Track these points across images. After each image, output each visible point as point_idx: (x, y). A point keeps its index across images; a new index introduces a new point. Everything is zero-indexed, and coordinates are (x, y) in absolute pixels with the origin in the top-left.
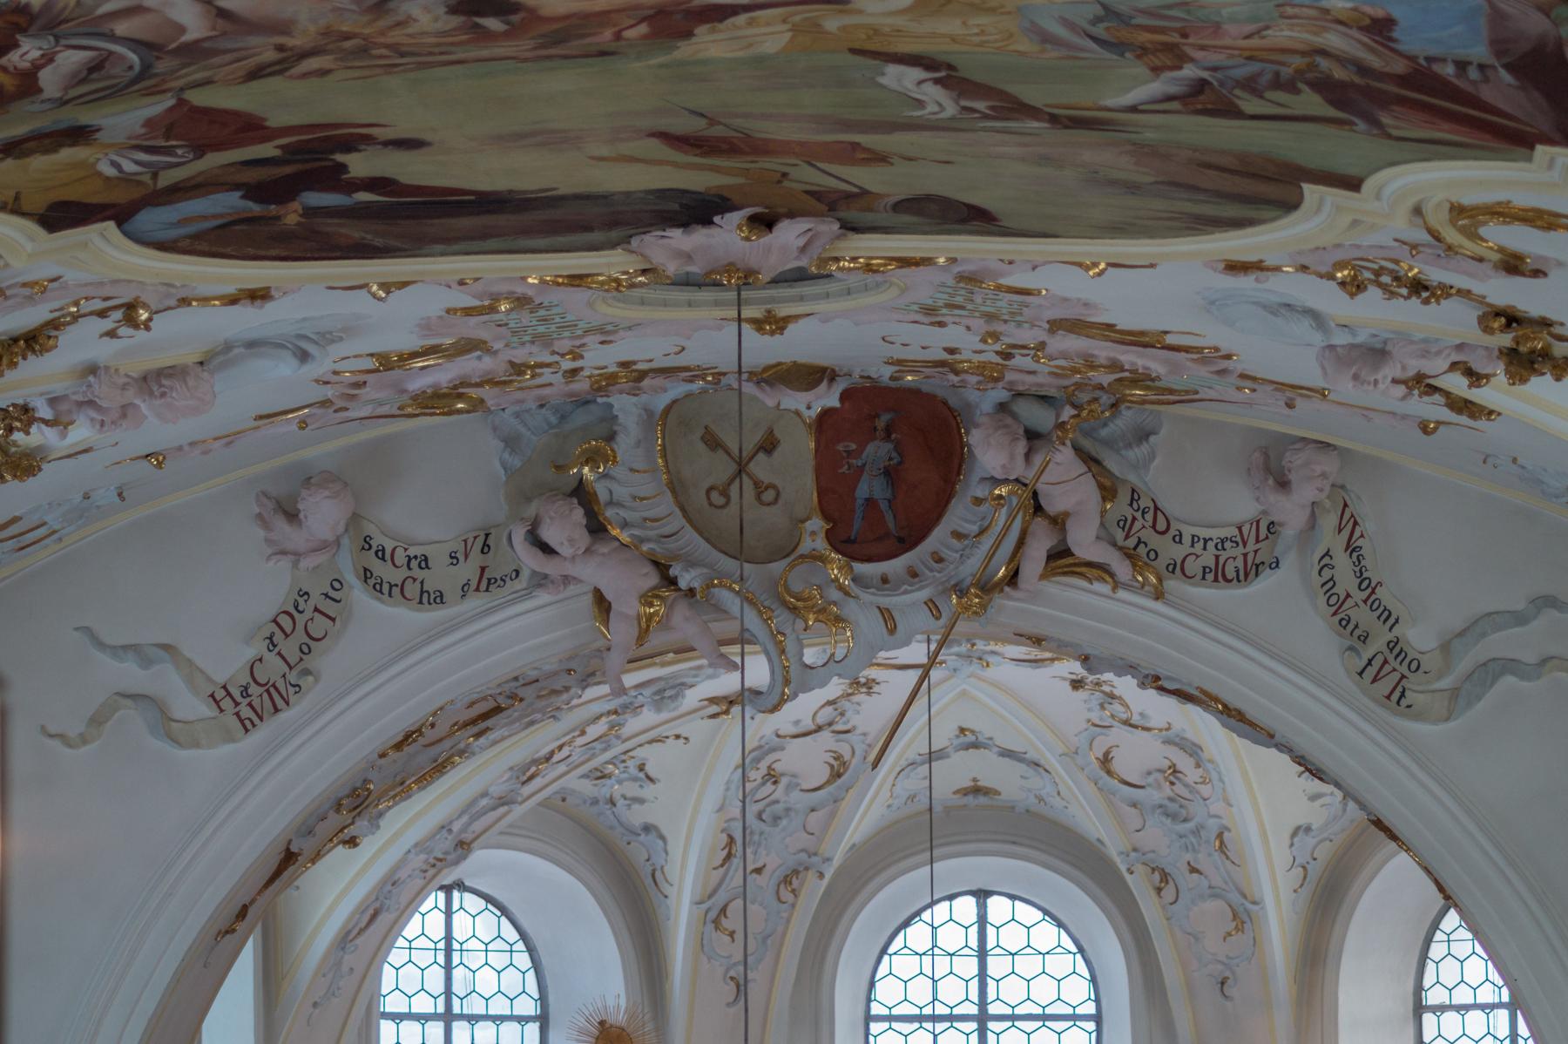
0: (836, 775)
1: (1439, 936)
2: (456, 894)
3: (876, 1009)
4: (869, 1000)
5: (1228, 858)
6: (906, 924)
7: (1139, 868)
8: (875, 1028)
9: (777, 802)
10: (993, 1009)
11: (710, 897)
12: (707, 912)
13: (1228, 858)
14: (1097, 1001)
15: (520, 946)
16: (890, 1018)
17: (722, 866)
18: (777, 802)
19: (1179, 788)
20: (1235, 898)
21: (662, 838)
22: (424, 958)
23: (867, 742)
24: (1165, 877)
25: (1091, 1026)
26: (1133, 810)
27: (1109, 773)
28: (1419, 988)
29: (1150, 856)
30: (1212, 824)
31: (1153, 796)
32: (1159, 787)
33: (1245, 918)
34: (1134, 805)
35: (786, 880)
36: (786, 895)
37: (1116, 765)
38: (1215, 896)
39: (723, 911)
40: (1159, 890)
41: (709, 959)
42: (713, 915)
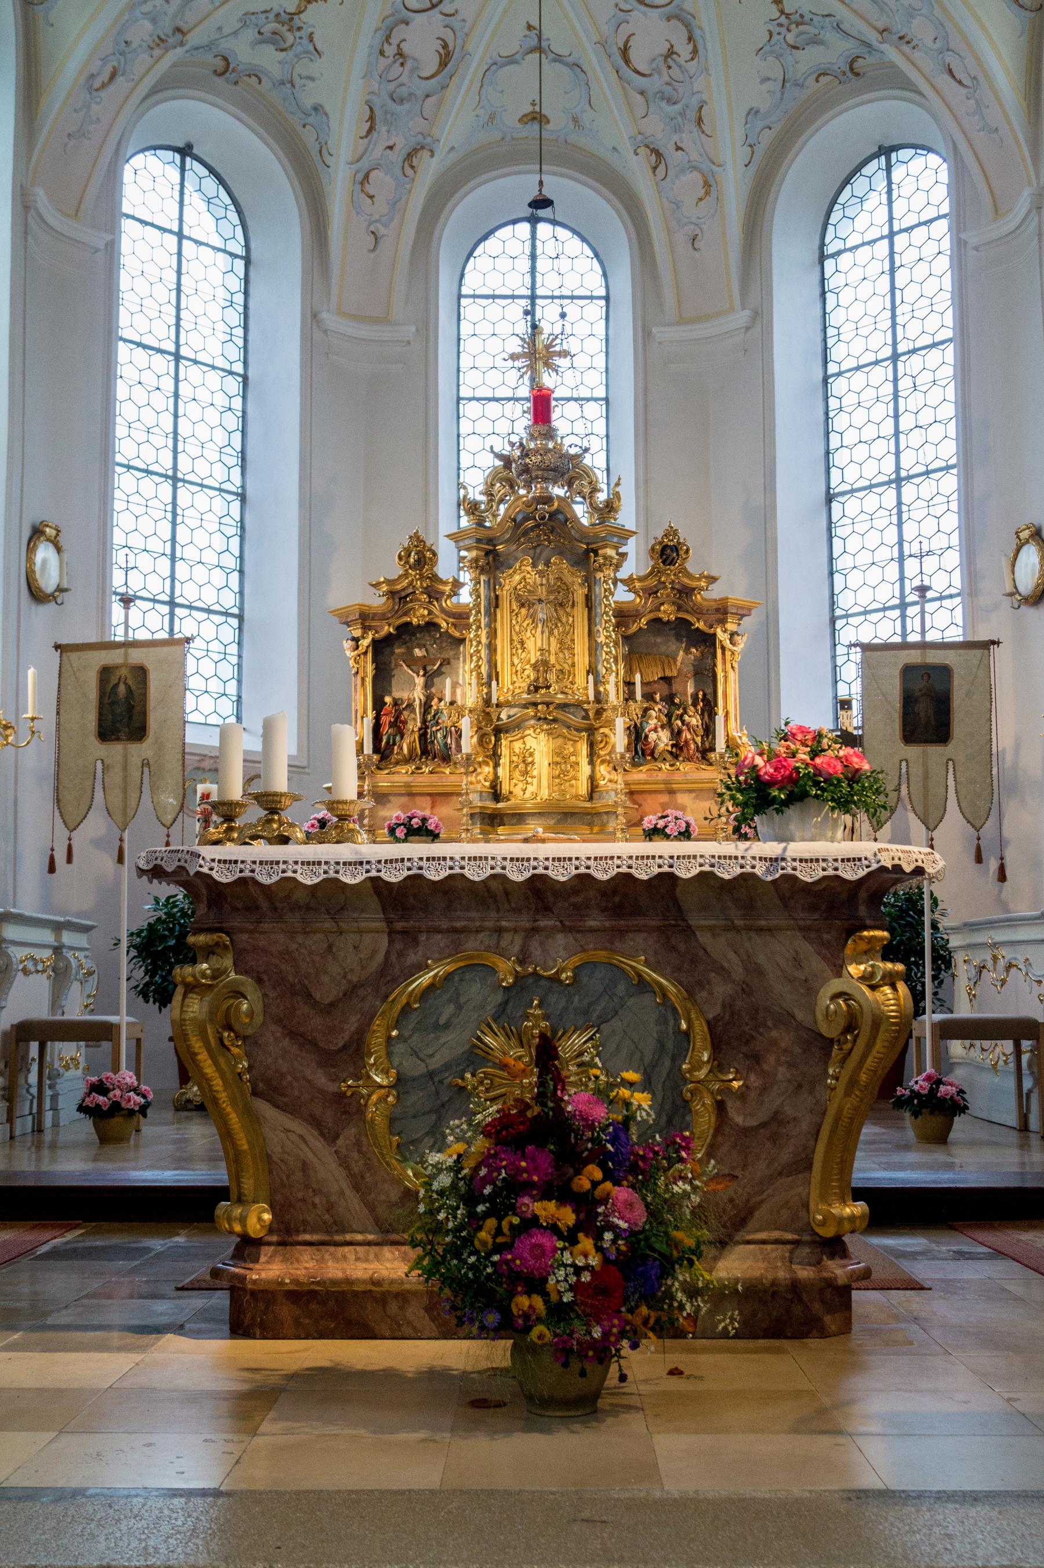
0: (443, 64)
1: (837, 207)
2: (188, 160)
3: (465, 291)
4: (460, 285)
5: (703, 132)
6: (485, 238)
7: (643, 151)
8: (464, 302)
9: (402, 85)
10: (539, 292)
11: (358, 161)
12: (357, 172)
13: (703, 132)
14: (607, 287)
15: (232, 208)
16: (474, 296)
17: (366, 137)
18: (402, 85)
19: (675, 72)
20: (706, 166)
21: (326, 114)
22: (166, 192)
23: (466, 30)
24: (658, 154)
25: (603, 303)
26: (639, 96)
27: (627, 61)
28: (822, 245)
29: (651, 139)
30: (694, 101)
31: (655, 84)
32: (660, 73)
33: (712, 182)
34: (642, 93)
35: (409, 156)
36: (409, 171)
37: (633, 54)
38: (695, 168)
39: (367, 176)
40: (655, 168)
41: (358, 213)
42: (360, 177)
